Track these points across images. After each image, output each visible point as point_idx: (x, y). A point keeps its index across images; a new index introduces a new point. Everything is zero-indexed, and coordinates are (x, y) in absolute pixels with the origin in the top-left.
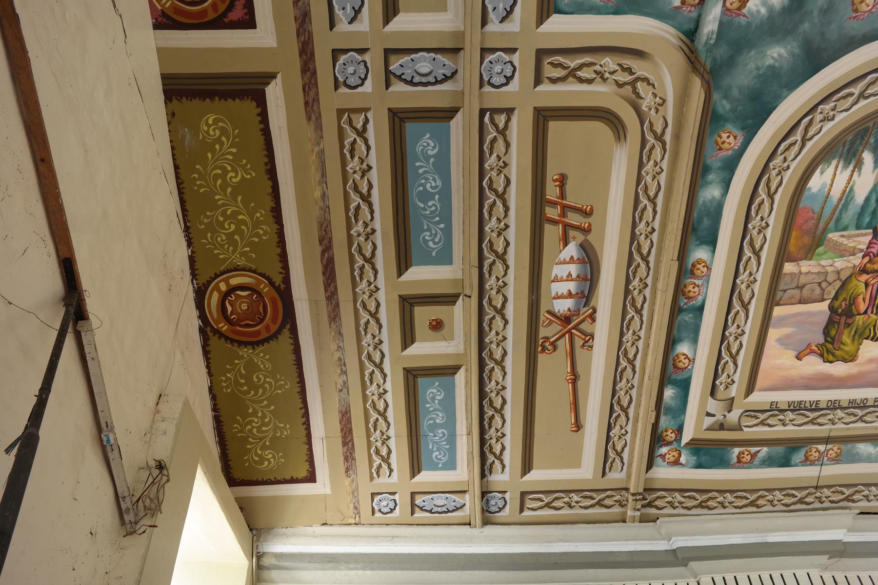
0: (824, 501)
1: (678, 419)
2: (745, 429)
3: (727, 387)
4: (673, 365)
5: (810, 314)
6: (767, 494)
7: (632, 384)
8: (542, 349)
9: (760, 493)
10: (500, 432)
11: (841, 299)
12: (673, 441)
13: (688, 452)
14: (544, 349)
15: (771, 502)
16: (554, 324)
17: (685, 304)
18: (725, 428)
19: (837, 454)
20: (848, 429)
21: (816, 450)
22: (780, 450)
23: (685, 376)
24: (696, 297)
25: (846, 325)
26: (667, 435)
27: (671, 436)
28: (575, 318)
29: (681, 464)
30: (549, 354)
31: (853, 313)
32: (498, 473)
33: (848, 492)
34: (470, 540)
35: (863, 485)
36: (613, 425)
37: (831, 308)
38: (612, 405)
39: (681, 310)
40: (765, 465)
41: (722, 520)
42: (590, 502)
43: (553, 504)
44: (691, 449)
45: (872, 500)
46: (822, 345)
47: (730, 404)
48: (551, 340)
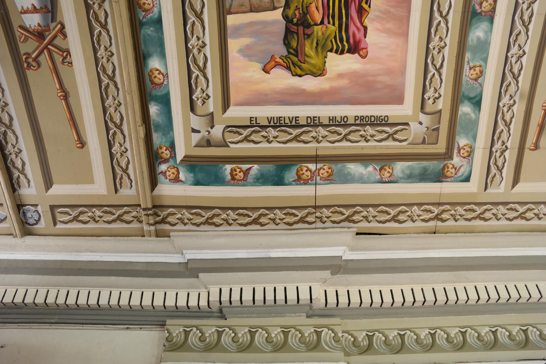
0: (326, 221)
1: (168, 136)
2: (232, 146)
3: (204, 103)
4: (150, 81)
5: (265, 23)
6: (268, 212)
7: (118, 101)
8: (28, 66)
9: (261, 211)
10: (16, 148)
11: (293, 7)
12: (169, 159)
13: (184, 169)
14: (29, 66)
15: (273, 220)
16: (30, 39)
17: (144, 17)
18: (212, 144)
19: (329, 174)
20: (335, 148)
21: (306, 168)
22: (270, 168)
23: (164, 92)
24: (151, 9)
25: (306, 36)
26: (163, 153)
27: (166, 154)
28: (47, 33)
29: (182, 181)
30: (36, 70)
31: (310, 23)
32: (26, 187)
33: (347, 213)
34: (13, 248)
35: (361, 206)
36: (112, 142)
37: (285, 17)
38: (106, 122)
39: (142, 24)
40: (259, 183)
41: (228, 235)
42: (111, 218)
43: (80, 218)
44: (186, 166)
45: (371, 221)
46: (286, 57)
47: (211, 118)
48: (33, 56)
